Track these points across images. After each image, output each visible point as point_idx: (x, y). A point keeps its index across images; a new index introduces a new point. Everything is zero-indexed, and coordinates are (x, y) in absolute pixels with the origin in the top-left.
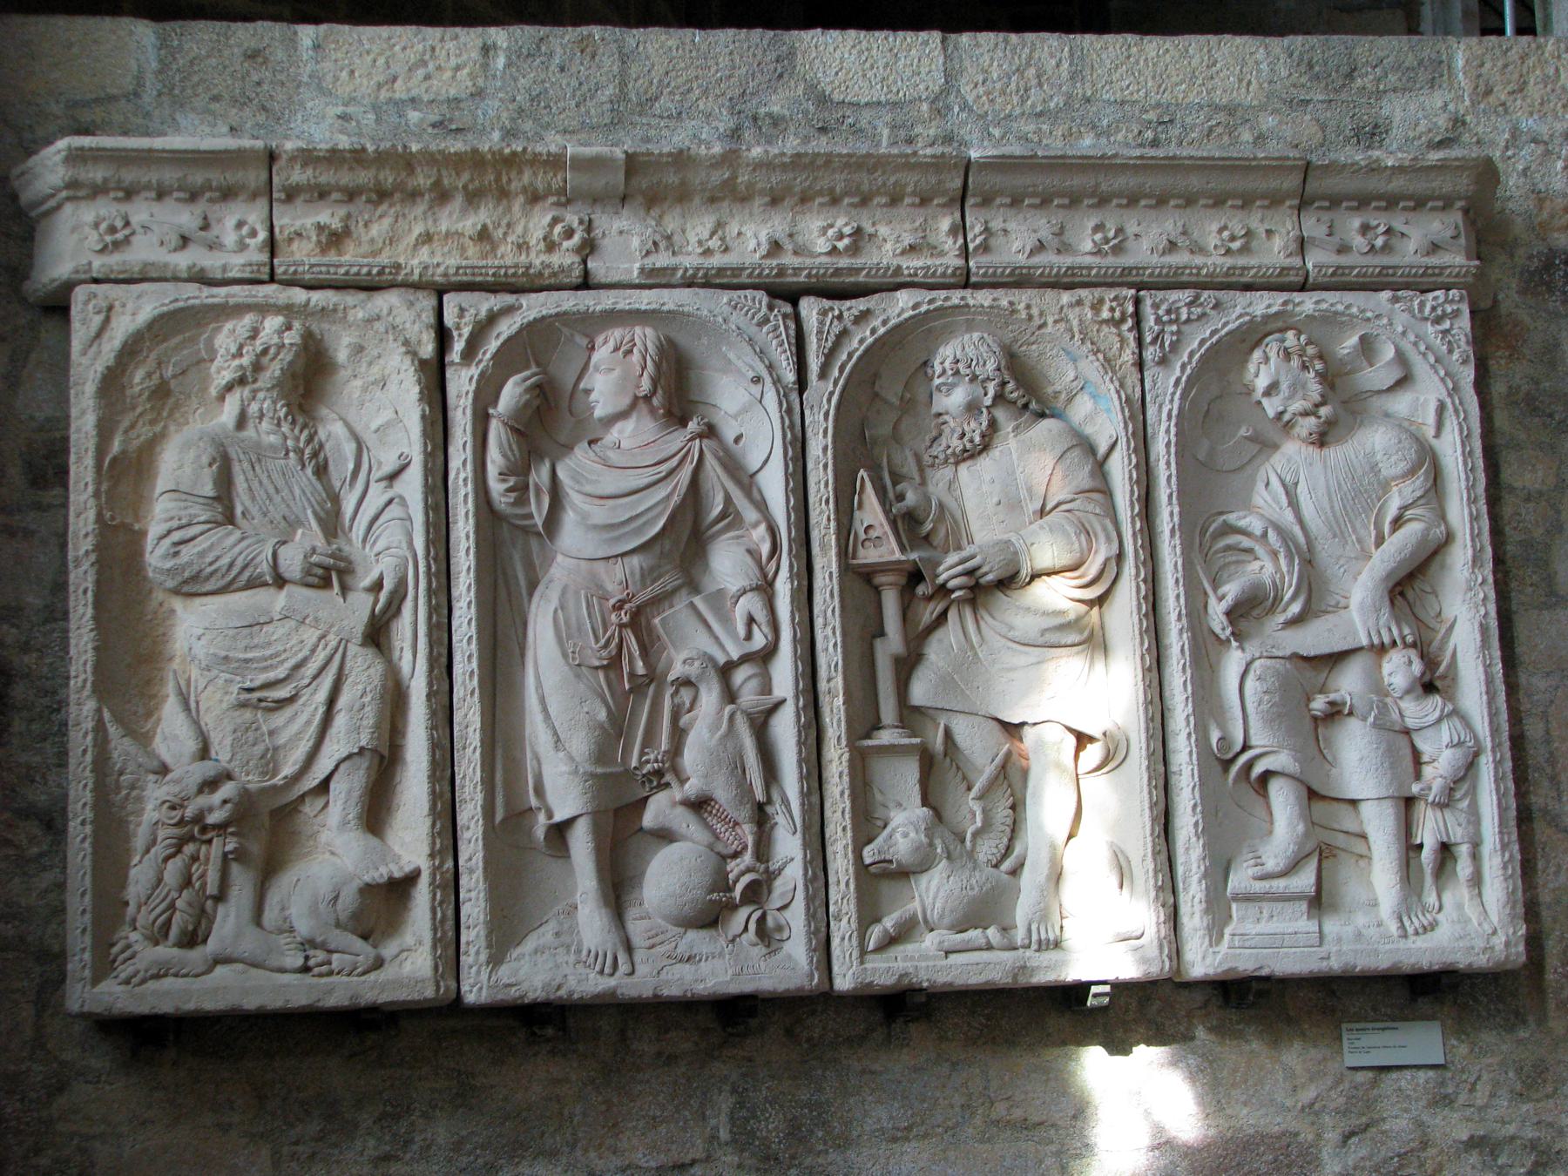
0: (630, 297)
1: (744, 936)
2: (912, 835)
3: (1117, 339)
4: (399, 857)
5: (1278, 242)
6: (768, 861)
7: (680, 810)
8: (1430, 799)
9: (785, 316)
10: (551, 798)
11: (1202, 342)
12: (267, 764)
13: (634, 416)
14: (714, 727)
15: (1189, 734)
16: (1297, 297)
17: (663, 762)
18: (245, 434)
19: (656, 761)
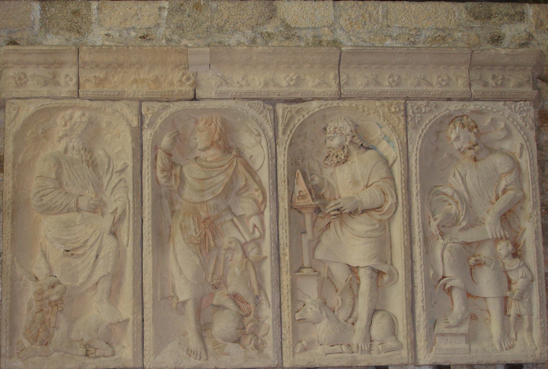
2: (314, 309)
3: (397, 119)
5: (460, 82)
7: (226, 298)
8: (514, 298)
9: (269, 110)
10: (178, 293)
11: (430, 120)
15: (421, 272)
16: (467, 103)
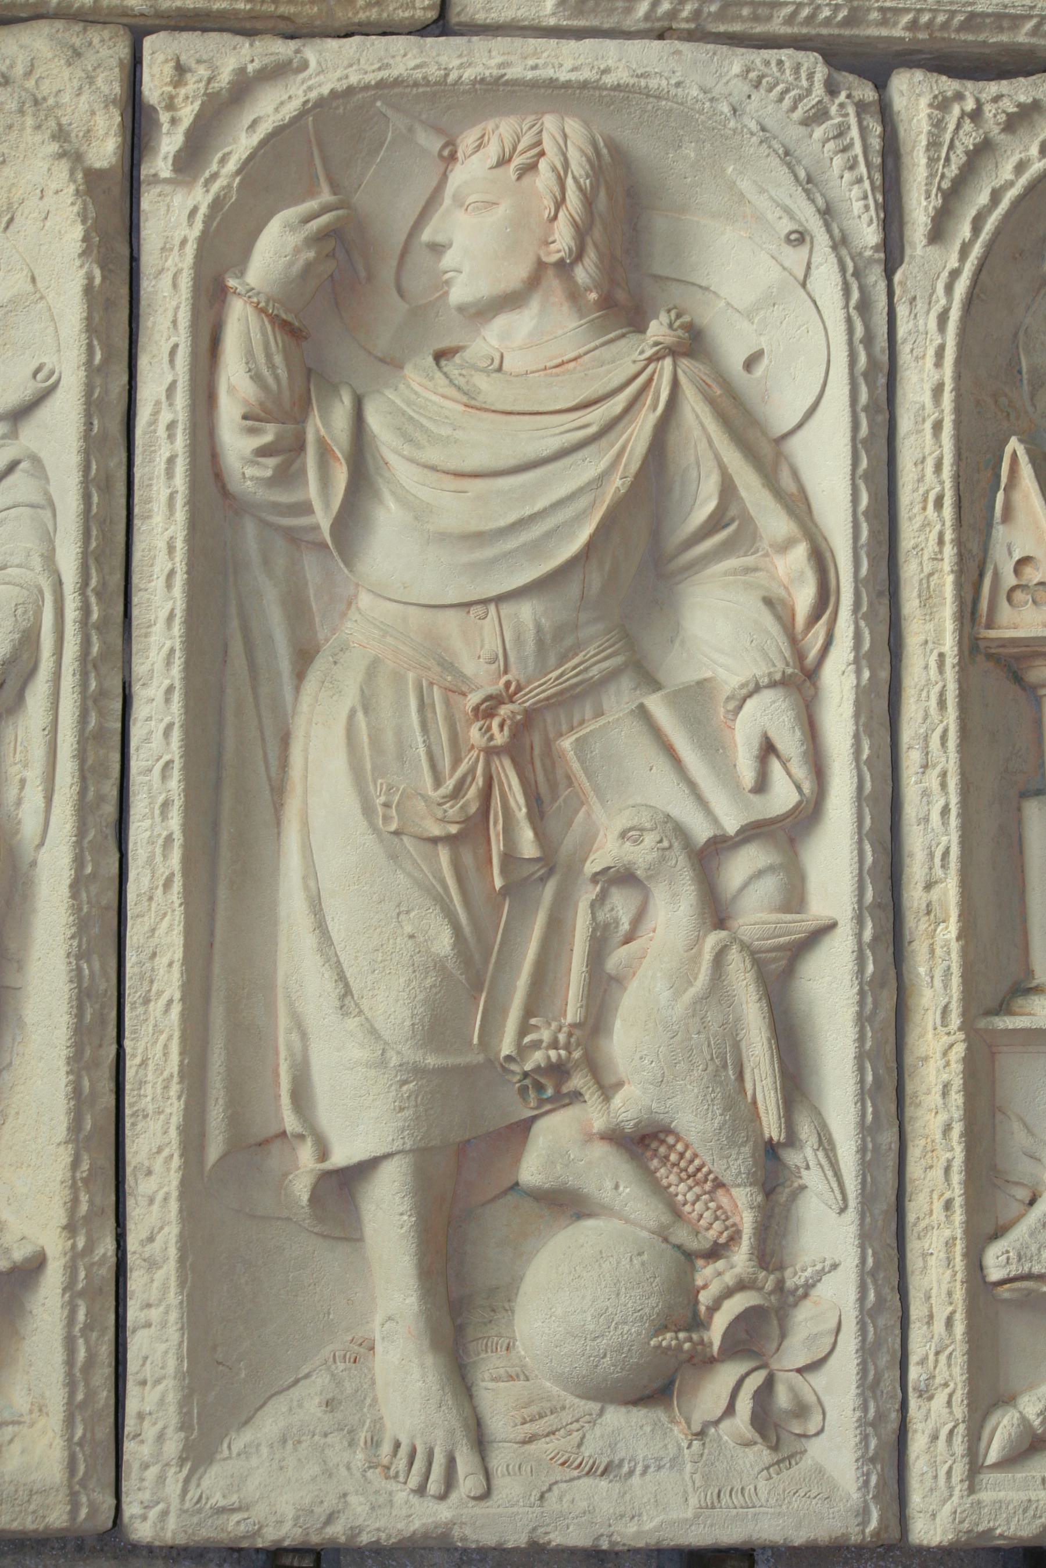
0: (535, 54)
1: (725, 1425)
6: (781, 1268)
7: (600, 1150)
9: (861, 108)
13: (534, 305)
14: (682, 979)
17: (567, 1047)
19: (554, 1045)
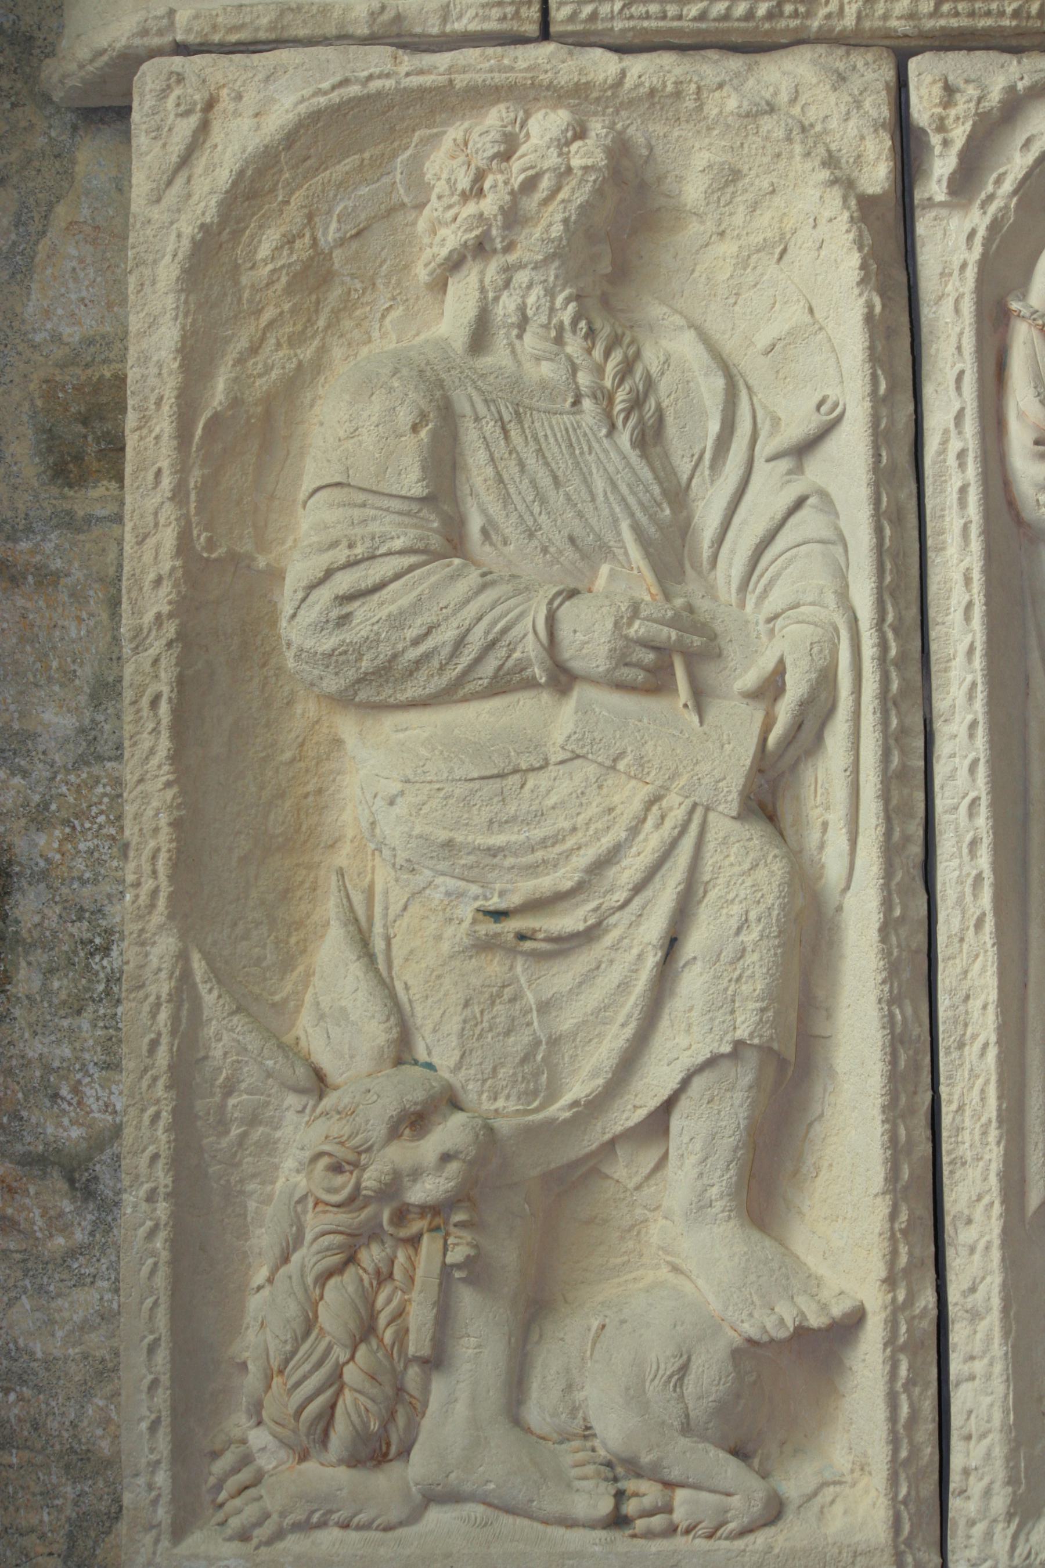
4: (819, 1282)
12: (536, 1075)
18: (487, 361)
